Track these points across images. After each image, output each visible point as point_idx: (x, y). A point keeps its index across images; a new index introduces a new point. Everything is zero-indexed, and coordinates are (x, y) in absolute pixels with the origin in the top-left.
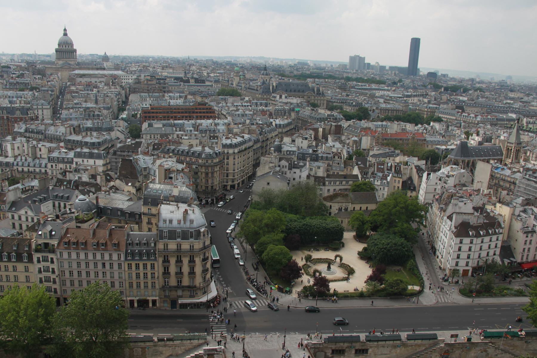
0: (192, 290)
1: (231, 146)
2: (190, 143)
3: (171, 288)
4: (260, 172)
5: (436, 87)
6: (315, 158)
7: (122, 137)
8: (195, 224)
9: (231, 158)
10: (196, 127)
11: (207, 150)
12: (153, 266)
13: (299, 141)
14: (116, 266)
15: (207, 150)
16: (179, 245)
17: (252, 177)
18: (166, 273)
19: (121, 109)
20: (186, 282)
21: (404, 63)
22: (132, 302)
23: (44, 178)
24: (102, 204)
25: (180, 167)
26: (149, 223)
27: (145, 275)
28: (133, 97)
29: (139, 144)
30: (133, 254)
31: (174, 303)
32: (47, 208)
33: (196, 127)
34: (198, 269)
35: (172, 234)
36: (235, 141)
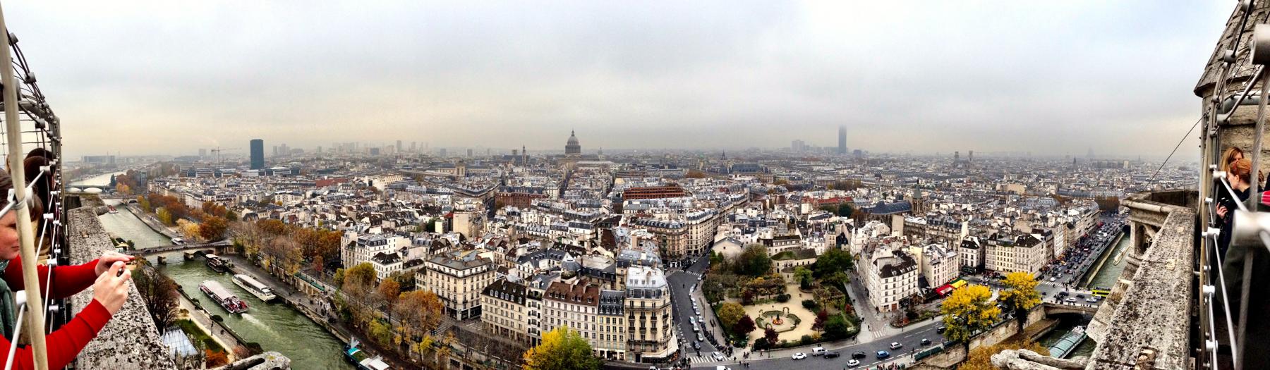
0: (654, 344)
1: (694, 218)
2: (662, 216)
3: (638, 343)
4: (717, 239)
5: (861, 161)
6: (763, 224)
7: (607, 212)
8: (657, 285)
9: (694, 230)
10: (667, 204)
11: (673, 222)
12: (621, 322)
13: (749, 211)
14: (590, 319)
15: (673, 222)
16: (643, 303)
17: (712, 244)
18: (632, 329)
19: (608, 191)
20: (648, 337)
21: (836, 144)
22: (602, 352)
23: (545, 240)
24: (585, 265)
25: (650, 236)
26: (622, 283)
27: (615, 328)
28: (618, 181)
29: (619, 218)
30: (604, 309)
31: (638, 357)
32: (544, 264)
33: (667, 204)
34: (660, 325)
35: (637, 293)
36: (697, 214)
